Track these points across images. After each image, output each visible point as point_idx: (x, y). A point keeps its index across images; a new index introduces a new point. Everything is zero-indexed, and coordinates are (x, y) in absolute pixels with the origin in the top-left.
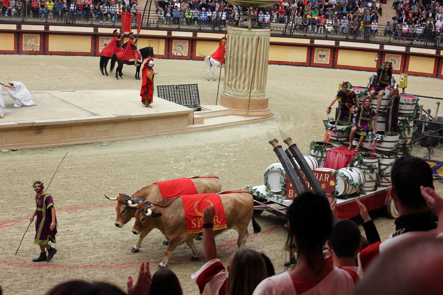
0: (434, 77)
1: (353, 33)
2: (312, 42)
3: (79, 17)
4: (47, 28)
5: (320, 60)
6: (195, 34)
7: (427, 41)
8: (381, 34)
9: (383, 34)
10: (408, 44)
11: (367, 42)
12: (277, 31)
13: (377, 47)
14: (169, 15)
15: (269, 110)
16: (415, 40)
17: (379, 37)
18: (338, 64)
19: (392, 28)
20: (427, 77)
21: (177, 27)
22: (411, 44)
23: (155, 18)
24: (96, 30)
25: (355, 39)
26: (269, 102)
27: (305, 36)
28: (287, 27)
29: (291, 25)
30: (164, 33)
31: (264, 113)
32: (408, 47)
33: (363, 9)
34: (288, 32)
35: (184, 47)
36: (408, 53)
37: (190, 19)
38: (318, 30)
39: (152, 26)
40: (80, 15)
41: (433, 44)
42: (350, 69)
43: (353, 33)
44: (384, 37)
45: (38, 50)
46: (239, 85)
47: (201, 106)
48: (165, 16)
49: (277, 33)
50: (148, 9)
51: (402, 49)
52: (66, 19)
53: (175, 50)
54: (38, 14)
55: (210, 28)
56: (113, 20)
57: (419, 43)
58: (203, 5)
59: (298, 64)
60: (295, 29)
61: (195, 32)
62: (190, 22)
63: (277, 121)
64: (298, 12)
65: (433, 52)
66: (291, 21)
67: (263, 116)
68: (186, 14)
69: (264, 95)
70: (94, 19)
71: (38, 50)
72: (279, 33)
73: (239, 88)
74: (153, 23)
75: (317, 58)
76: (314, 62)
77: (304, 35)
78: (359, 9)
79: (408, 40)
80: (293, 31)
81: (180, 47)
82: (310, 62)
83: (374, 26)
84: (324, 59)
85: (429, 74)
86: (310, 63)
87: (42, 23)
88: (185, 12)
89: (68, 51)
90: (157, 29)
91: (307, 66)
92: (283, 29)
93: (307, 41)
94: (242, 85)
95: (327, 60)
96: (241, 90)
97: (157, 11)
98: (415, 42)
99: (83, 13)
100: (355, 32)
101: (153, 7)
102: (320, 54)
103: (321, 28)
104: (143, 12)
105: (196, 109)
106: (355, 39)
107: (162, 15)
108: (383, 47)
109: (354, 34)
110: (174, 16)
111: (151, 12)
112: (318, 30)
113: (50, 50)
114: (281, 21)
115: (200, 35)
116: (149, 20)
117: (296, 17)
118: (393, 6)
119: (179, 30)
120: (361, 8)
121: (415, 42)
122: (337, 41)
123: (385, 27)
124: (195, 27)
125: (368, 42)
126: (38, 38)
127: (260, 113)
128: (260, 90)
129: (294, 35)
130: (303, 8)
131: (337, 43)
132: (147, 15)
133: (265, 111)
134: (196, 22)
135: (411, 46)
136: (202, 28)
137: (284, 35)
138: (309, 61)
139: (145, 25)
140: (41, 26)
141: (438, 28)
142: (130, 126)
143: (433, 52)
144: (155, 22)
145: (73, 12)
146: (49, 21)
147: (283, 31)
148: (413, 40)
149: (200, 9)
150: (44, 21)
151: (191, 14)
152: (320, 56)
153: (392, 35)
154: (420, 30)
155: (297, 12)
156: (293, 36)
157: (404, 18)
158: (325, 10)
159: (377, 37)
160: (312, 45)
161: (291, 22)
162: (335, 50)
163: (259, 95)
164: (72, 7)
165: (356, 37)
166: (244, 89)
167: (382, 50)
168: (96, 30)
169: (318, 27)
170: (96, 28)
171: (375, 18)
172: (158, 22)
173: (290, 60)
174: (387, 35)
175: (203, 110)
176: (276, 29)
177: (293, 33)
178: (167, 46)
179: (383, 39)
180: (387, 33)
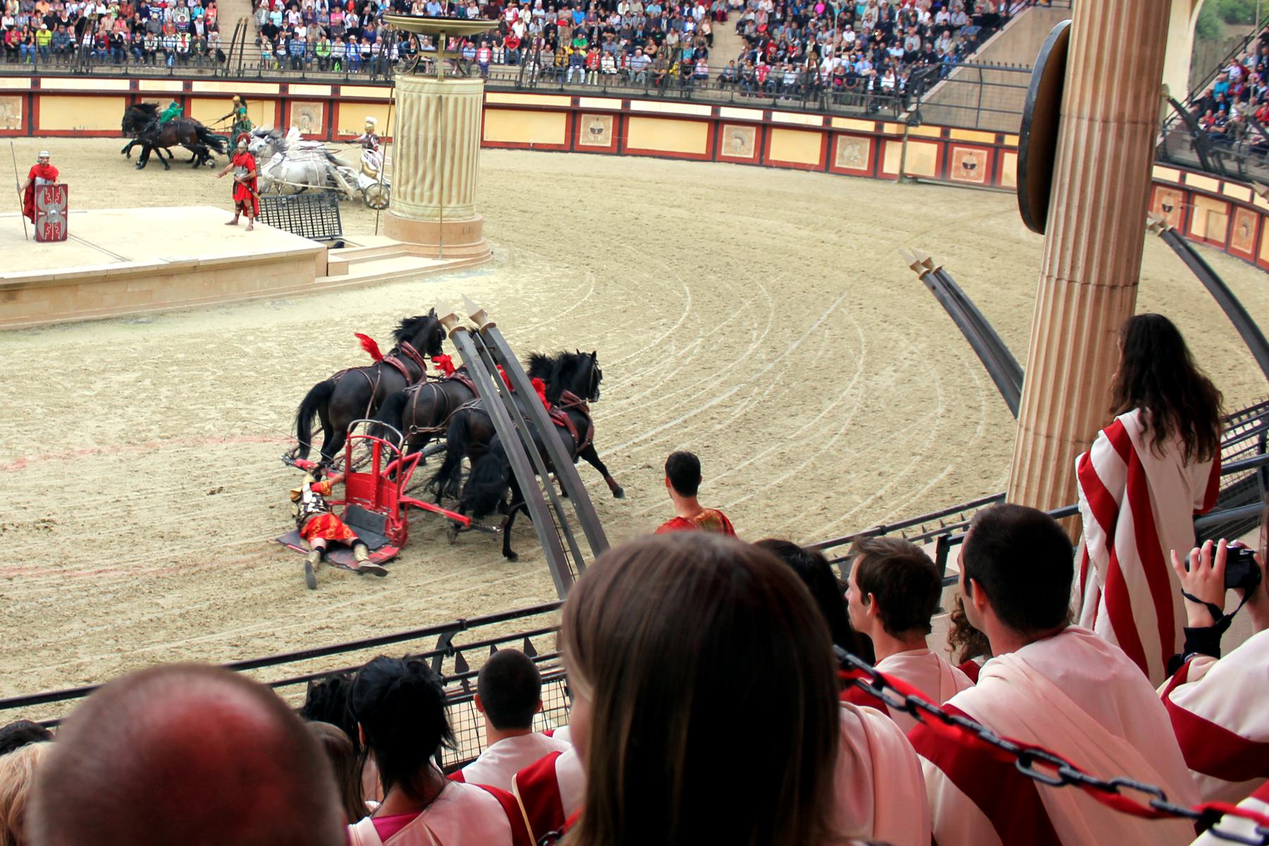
0: (821, 172)
2: (575, 102)
3: (101, 59)
4: (36, 83)
6: (336, 90)
12: (503, 80)
13: (706, 111)
14: (283, 52)
21: (298, 75)
22: (774, 105)
23: (254, 57)
24: (134, 85)
26: (485, 227)
27: (561, 90)
29: (531, 69)
30: (274, 89)
31: (473, 251)
32: (768, 110)
33: (676, 37)
34: (526, 83)
35: (314, 116)
37: (327, 59)
38: (586, 77)
39: (248, 74)
40: (103, 55)
41: (817, 105)
42: (654, 157)
44: (719, 92)
45: (19, 127)
46: (422, 195)
47: (346, 236)
48: (274, 53)
49: (504, 84)
50: (240, 41)
51: (757, 115)
52: (74, 63)
53: (295, 122)
54: (17, 56)
55: (367, 78)
56: (170, 63)
58: (351, 31)
60: (542, 75)
61: (336, 86)
62: (327, 63)
63: (501, 266)
64: (547, 42)
65: (817, 121)
67: (471, 255)
68: (318, 49)
70: (131, 62)
71: (19, 127)
73: (422, 200)
74: (251, 69)
75: (585, 134)
76: (581, 143)
78: (669, 36)
79: (766, 97)
81: (307, 117)
82: (572, 144)
83: (700, 68)
84: (600, 137)
85: (811, 165)
86: (571, 145)
87: (27, 72)
88: (315, 46)
89: (78, 128)
90: (259, 80)
91: (567, 152)
93: (565, 102)
94: (427, 194)
95: (606, 140)
96: (425, 203)
97: (259, 43)
98: (782, 101)
99: (109, 52)
100: (661, 81)
101: (251, 37)
102: (592, 126)
103: (593, 75)
104: (229, 46)
105: (334, 243)
106: (662, 96)
107: (268, 52)
110: (293, 53)
111: (245, 47)
112: (586, 77)
113: (43, 126)
114: (511, 61)
115: (346, 91)
116: (243, 62)
117: (542, 52)
118: (737, 28)
119: (303, 81)
120: (673, 35)
122: (626, 99)
123: (721, 71)
124: (335, 74)
125: (689, 101)
126: (19, 102)
127: (465, 251)
128: (464, 202)
129: (539, 89)
130: (556, 32)
131: (626, 104)
132: (239, 52)
134: (337, 66)
136: (350, 77)
137: (518, 89)
139: (233, 72)
140: (25, 79)
142: (198, 280)
143: (817, 121)
144: (255, 67)
145: (88, 50)
146: (40, 69)
147: (515, 82)
148: (778, 97)
149: (345, 39)
150: (31, 69)
151: (328, 49)
152: (593, 130)
153: (737, 88)
154: (790, 78)
155: (543, 42)
157: (759, 55)
158: (601, 38)
160: (575, 108)
161: (532, 63)
162: (622, 118)
164: (87, 41)
166: (430, 201)
168: (134, 85)
169: (587, 72)
170: (135, 80)
171: (701, 54)
172: (260, 66)
173: (532, 141)
175: (349, 246)
178: (279, 115)
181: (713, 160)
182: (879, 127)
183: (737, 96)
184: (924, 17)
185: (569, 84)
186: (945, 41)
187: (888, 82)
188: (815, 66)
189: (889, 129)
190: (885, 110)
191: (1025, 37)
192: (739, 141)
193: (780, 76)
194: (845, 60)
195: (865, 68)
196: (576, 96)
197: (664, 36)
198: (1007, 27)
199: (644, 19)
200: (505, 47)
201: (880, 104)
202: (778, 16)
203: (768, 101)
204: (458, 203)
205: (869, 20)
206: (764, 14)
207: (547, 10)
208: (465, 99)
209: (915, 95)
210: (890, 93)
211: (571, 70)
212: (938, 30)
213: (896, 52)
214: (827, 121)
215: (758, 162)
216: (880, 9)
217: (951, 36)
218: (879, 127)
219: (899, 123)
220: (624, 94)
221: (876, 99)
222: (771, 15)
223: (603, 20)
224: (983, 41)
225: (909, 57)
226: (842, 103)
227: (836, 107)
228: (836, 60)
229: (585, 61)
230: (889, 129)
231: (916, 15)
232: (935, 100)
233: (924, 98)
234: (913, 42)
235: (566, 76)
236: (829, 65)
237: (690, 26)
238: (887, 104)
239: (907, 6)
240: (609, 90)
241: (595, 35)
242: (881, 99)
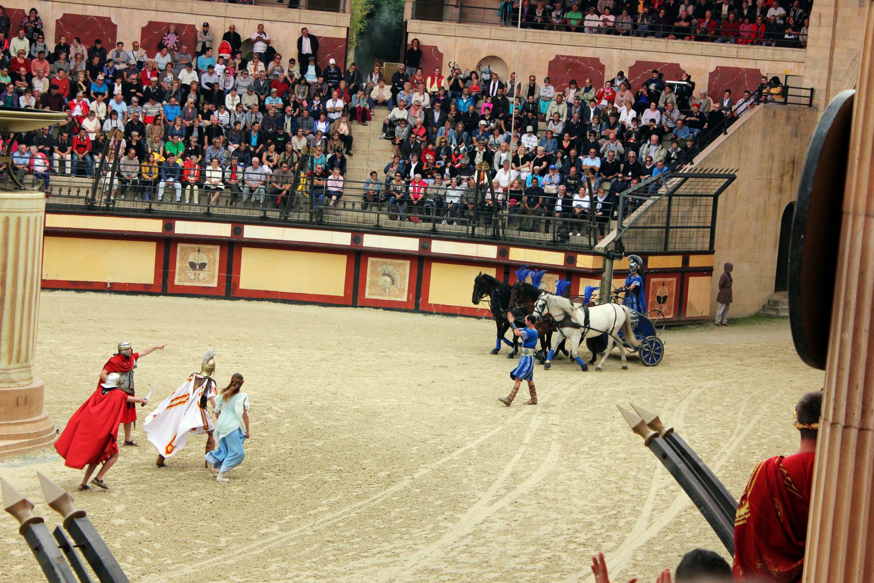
1: (279, 202)
2: (169, 228)
5: (193, 277)
7: (474, 223)
8: (354, 205)
9: (358, 206)
10: (426, 232)
11: (317, 226)
12: (69, 196)
13: (344, 239)
15: (45, 419)
16: (443, 220)
17: (349, 213)
18: (241, 287)
19: (383, 187)
20: (479, 318)
22: (434, 231)
25: (286, 218)
26: (47, 397)
27: (150, 210)
28: (99, 186)
29: (108, 181)
31: (31, 429)
32: (426, 238)
33: (304, 141)
34: (100, 201)
36: (426, 254)
38: (183, 193)
42: (275, 301)
43: (279, 202)
44: (361, 214)
49: (70, 202)
51: (411, 245)
57: (455, 228)
59: (132, 289)
60: (122, 190)
64: (129, 145)
66: (107, 171)
67: (28, 436)
69: (31, 378)
72: (75, 202)
75: (183, 269)
76: (177, 282)
77: (146, 209)
78: (294, 139)
79: (425, 220)
80: (115, 197)
82: (165, 283)
83: (333, 183)
84: (202, 274)
91: (157, 294)
92: (87, 192)
93: (155, 226)
95: (210, 278)
98: (443, 226)
100: (284, 200)
102: (191, 259)
108: (361, 240)
109: (282, 204)
112: (183, 193)
114: (80, 170)
117: (124, 159)
118: (384, 130)
120: (300, 138)
121: (443, 226)
122: (238, 224)
123: (362, 185)
127: (20, 430)
129: (119, 210)
130: (142, 133)
131: (237, 231)
133: (34, 422)
135: (432, 236)
137: (90, 209)
138: (161, 281)
141: (500, 190)
147: (86, 198)
148: (439, 221)
152: (193, 265)
153: (385, 209)
154: (454, 196)
155: (124, 143)
156: (115, 213)
157: (414, 166)
159: (343, 213)
160: (168, 234)
161: (109, 174)
163: (14, 377)
165: (287, 213)
167: (359, 249)
169: (184, 186)
173: (109, 279)
174: (369, 209)
176: (67, 193)
177: (114, 202)
179: (361, 220)
180: (371, 200)
181: (354, 305)
182: (570, 260)
183: (384, 219)
184: (627, 116)
185: (161, 202)
186: (653, 148)
187: (581, 201)
188: (486, 180)
189: (584, 262)
190: (578, 238)
191: (755, 142)
192: (388, 279)
193: (441, 192)
194: (526, 172)
195: (551, 184)
196: (169, 219)
197: (288, 139)
198: (731, 130)
199: (260, 116)
200: (72, 153)
201: (572, 230)
202: (437, 116)
203: (429, 226)
204: (10, 362)
205: (557, 120)
206: (420, 110)
207: (129, 103)
208: (19, 219)
209: (616, 219)
210: (583, 214)
211: (162, 184)
212: (645, 133)
213: (590, 162)
214: (503, 253)
215: (412, 306)
216: (570, 105)
217: (660, 142)
218: (570, 260)
219: (596, 254)
220: (236, 217)
221: (565, 223)
222: (428, 113)
223: (206, 117)
224: (702, 148)
225: (607, 169)
226: (520, 229)
227: (513, 233)
228: (514, 173)
229: (182, 171)
230: (584, 262)
231: (618, 115)
232: (641, 223)
233: (627, 222)
234: (613, 148)
235: (156, 191)
236: (504, 178)
237: (322, 126)
238: (579, 230)
239: (604, 102)
240: (215, 211)
241: (194, 138)
242: (572, 223)
